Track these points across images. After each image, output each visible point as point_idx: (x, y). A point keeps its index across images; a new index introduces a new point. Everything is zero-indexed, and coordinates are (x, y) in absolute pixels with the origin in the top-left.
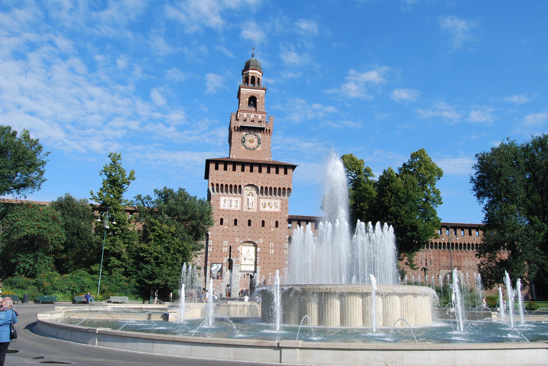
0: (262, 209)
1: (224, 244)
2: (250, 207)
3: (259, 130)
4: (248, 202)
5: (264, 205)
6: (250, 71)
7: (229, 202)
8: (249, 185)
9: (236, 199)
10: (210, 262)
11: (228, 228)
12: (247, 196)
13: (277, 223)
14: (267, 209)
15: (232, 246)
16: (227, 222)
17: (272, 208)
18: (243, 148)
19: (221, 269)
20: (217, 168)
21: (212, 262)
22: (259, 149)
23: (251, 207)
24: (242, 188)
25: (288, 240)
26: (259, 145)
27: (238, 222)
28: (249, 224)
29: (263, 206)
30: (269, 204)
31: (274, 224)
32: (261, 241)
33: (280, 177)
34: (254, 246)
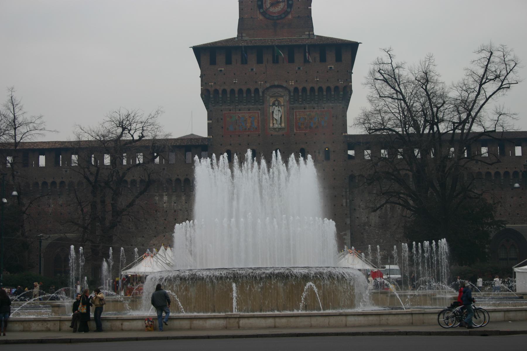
2: (276, 126)
4: (273, 117)
18: (261, 17)
20: (213, 62)
22: (290, 16)
24: (261, 94)
26: (289, 10)
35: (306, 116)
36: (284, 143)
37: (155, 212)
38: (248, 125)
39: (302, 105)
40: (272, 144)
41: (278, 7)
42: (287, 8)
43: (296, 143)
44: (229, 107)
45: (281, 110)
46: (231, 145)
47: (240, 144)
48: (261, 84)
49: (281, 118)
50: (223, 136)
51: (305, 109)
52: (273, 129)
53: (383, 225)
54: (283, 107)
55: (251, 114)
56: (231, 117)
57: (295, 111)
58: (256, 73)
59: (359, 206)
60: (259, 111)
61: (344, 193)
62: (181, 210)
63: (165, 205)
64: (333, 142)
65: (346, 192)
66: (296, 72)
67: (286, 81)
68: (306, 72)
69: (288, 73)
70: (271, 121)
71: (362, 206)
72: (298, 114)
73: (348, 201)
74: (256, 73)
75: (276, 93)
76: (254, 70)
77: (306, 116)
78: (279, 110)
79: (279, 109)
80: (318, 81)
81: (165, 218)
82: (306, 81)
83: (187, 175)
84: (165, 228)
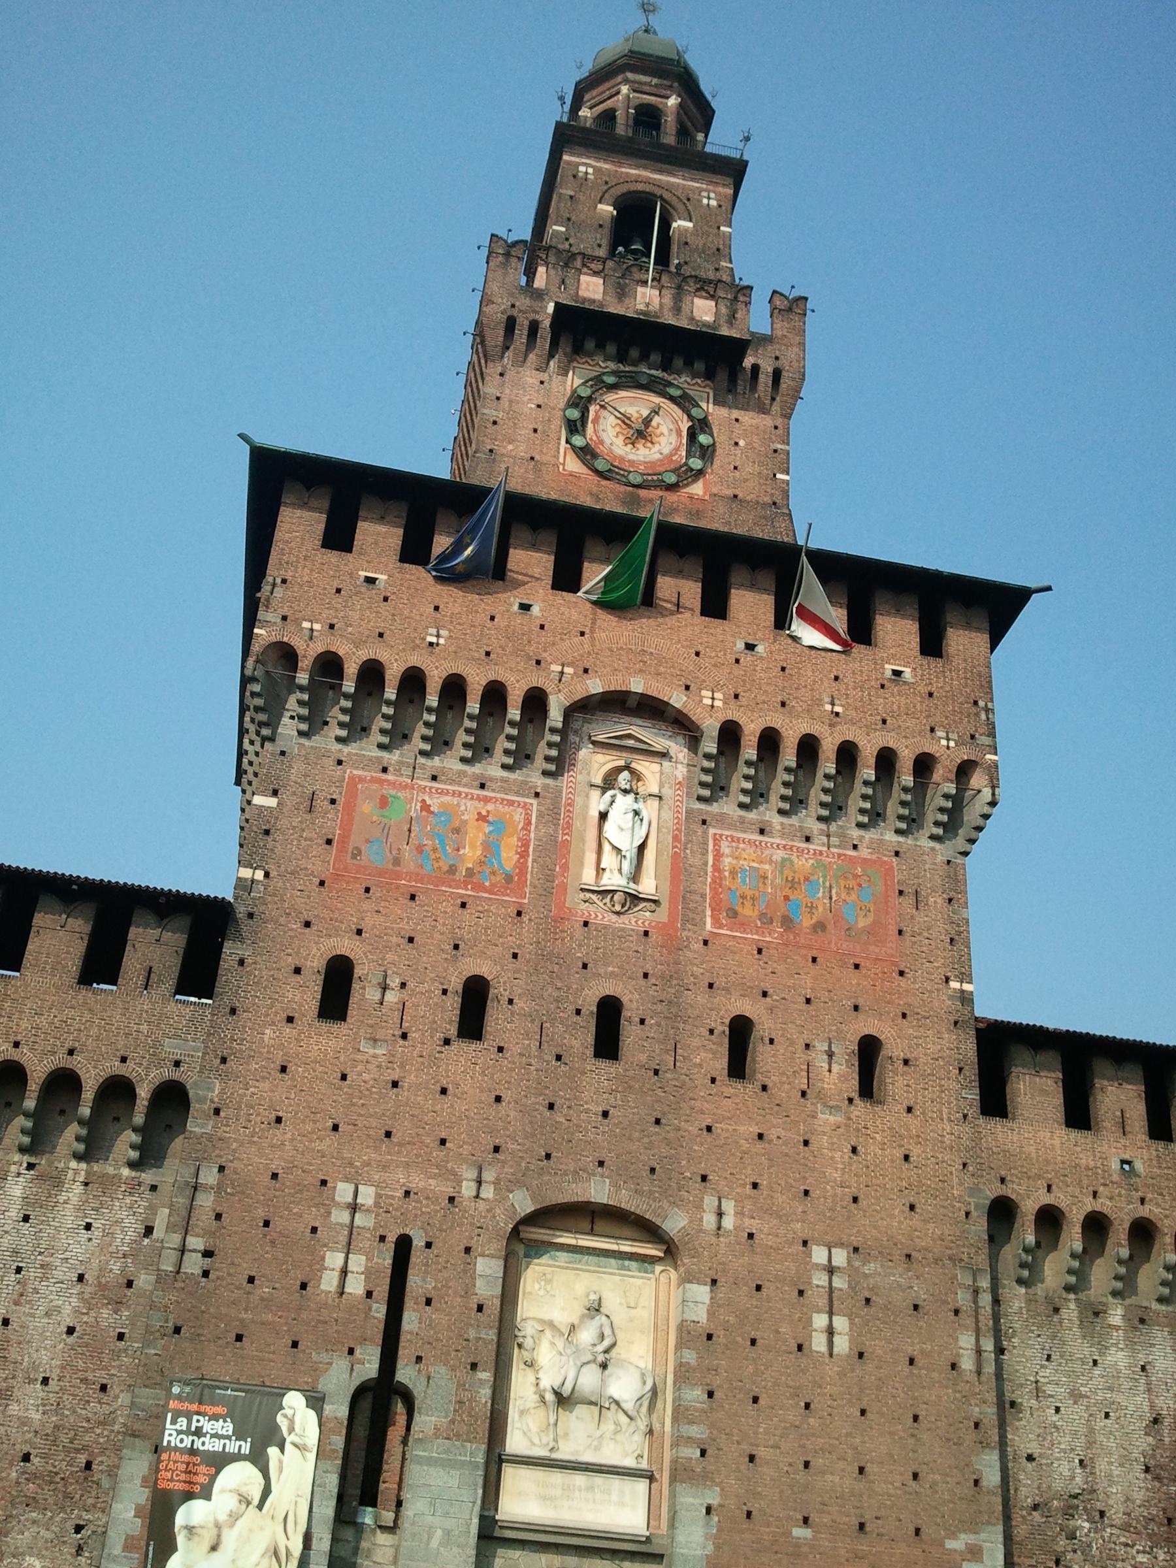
3: (699, 366)
6: (630, 75)
18: (573, 465)
22: (697, 489)
23: (632, 888)
24: (555, 716)
26: (696, 463)
33: (889, 667)
35: (767, 867)
36: (646, 975)
38: (466, 851)
39: (752, 815)
40: (585, 966)
41: (650, 449)
42: (689, 455)
43: (711, 986)
44: (384, 755)
45: (644, 814)
46: (359, 932)
47: (411, 940)
48: (562, 673)
49: (642, 848)
50: (322, 883)
51: (762, 832)
52: (594, 897)
54: (655, 803)
55: (490, 807)
56: (384, 802)
57: (712, 831)
58: (542, 627)
59: (1038, 1391)
60: (534, 802)
61: (963, 1299)
65: (976, 1292)
66: (737, 661)
67: (687, 688)
68: (783, 669)
69: (697, 654)
70: (590, 858)
71: (1050, 1389)
72: (725, 848)
74: (542, 627)
76: (536, 610)
77: (767, 867)
79: (636, 806)
80: (837, 714)
82: (783, 704)
83: (71, 1052)
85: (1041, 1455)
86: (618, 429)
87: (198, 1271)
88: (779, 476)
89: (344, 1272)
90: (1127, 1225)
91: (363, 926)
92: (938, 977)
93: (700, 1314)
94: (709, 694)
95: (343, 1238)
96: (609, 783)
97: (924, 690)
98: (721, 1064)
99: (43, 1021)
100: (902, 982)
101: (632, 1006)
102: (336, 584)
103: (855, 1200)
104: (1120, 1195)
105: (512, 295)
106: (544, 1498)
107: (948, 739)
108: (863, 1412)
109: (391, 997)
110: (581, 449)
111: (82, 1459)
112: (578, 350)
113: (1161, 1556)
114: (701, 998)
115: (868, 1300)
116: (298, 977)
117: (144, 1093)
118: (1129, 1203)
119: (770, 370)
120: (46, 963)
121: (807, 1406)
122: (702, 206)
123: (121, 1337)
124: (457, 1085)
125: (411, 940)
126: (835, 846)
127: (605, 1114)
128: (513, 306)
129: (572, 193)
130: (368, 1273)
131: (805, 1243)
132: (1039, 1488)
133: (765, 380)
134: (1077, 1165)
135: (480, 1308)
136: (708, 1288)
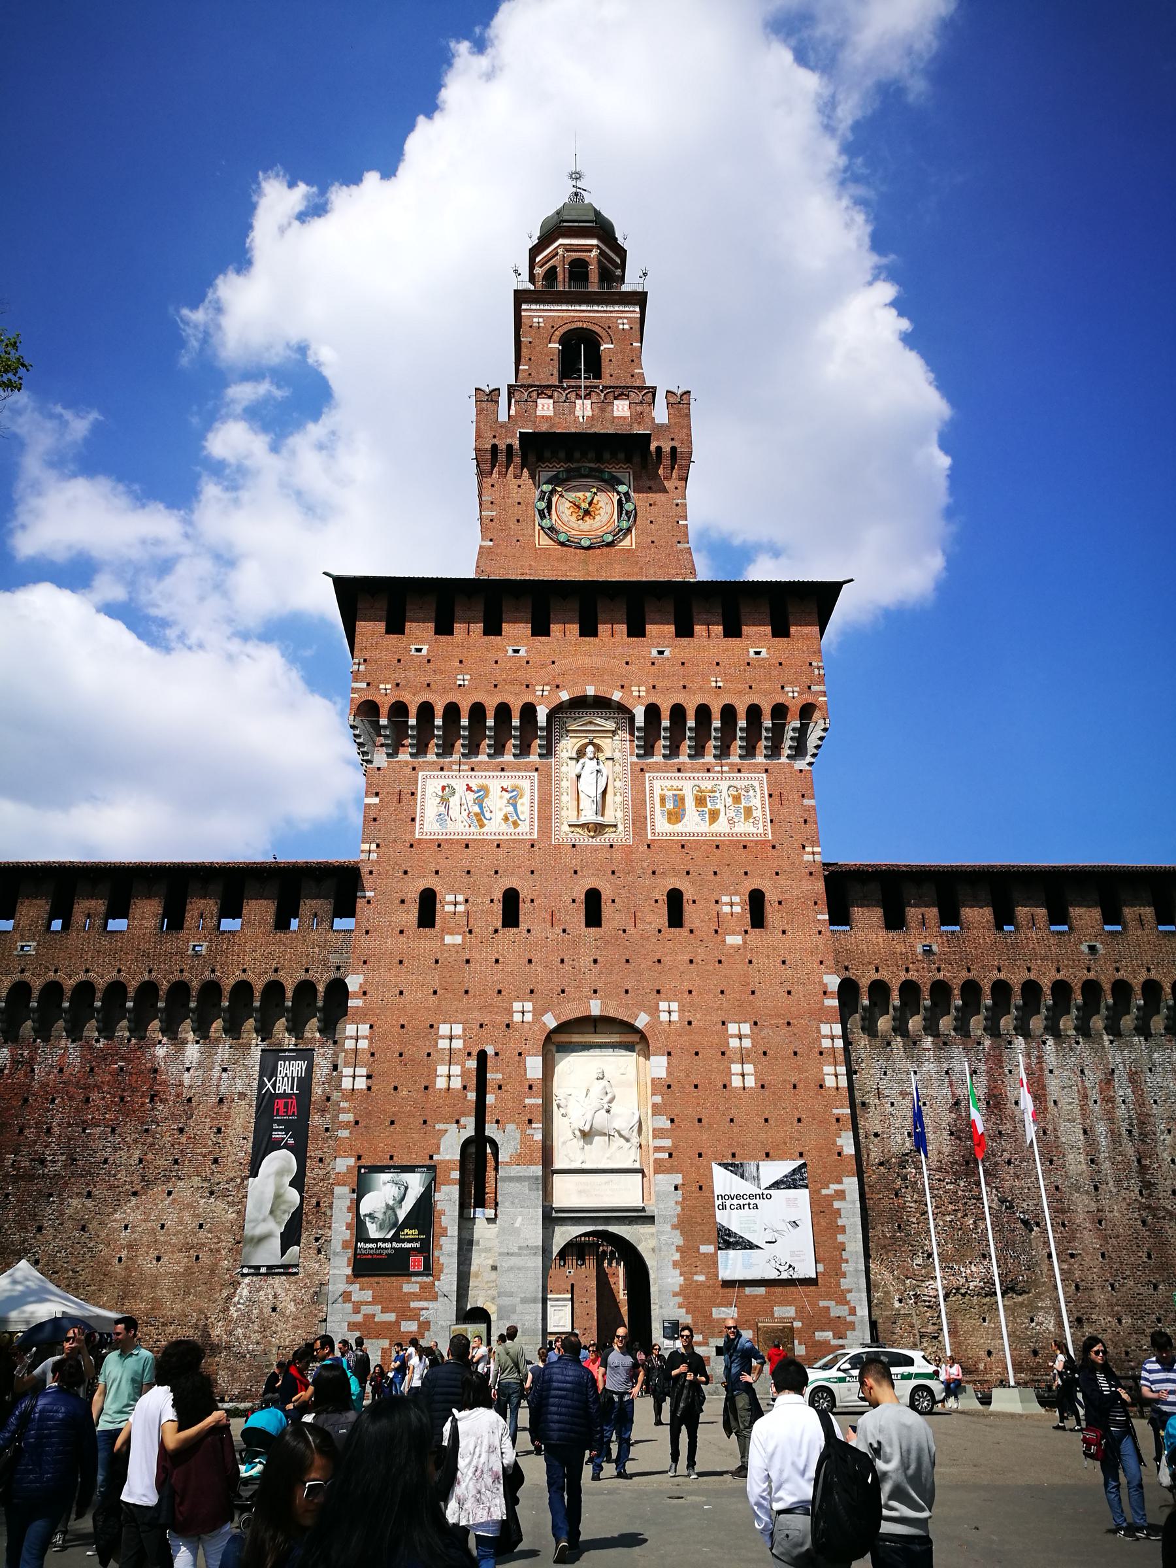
0: (661, 826)
1: (443, 1044)
3: (621, 456)
5: (670, 805)
7: (471, 796)
8: (580, 704)
9: (506, 783)
10: (352, 1161)
11: (463, 947)
12: (574, 762)
13: (756, 900)
14: (693, 824)
15: (490, 1051)
16: (461, 908)
17: (722, 818)
18: (544, 541)
19: (425, 1205)
21: (363, 1162)
22: (626, 543)
23: (599, 819)
24: (542, 719)
25: (835, 1002)
27: (524, 908)
28: (593, 917)
29: (669, 813)
30: (700, 801)
31: (734, 905)
32: (670, 1011)
33: (752, 651)
34: (630, 1047)
37: (147, 1101)
40: (575, 872)
43: (654, 873)
45: (605, 771)
46: (437, 872)
47: (469, 872)
49: (604, 792)
50: (411, 846)
52: (578, 830)
53: (967, 1163)
57: (647, 775)
58: (528, 662)
59: (879, 1095)
60: (536, 774)
62: (242, 1095)
63: (186, 1075)
64: (777, 874)
66: (653, 664)
68: (683, 664)
69: (627, 663)
71: (886, 1092)
73: (842, 1070)
74: (528, 662)
75: (591, 723)
76: (522, 653)
78: (598, 771)
79: (598, 768)
80: (720, 687)
81: (180, 1125)
83: (276, 970)
84: (176, 1162)
85: (883, 1133)
86: (572, 510)
87: (364, 1087)
88: (680, 522)
89: (449, 1077)
90: (928, 986)
91: (438, 868)
92: (797, 845)
93: (663, 1075)
94: (637, 688)
95: (447, 1058)
96: (581, 753)
97: (775, 662)
98: (664, 920)
99: (257, 955)
100: (774, 852)
101: (606, 893)
102: (397, 657)
103: (753, 992)
104: (923, 968)
105: (492, 429)
106: (580, 1192)
107: (793, 692)
108: (766, 1120)
109: (461, 908)
110: (549, 529)
111: (314, 1201)
112: (540, 459)
113: (962, 1184)
114: (648, 881)
115: (765, 1053)
116: (404, 905)
117: (321, 988)
118: (930, 972)
119: (668, 449)
120: (255, 920)
121: (732, 1120)
122: (619, 330)
123: (327, 1130)
124: (504, 957)
125: (469, 872)
126: (726, 772)
127: (595, 961)
128: (494, 437)
129: (530, 340)
130: (463, 1074)
131: (724, 1023)
132: (882, 1152)
133: (666, 458)
134: (894, 953)
135: (530, 1087)
136: (665, 1058)
